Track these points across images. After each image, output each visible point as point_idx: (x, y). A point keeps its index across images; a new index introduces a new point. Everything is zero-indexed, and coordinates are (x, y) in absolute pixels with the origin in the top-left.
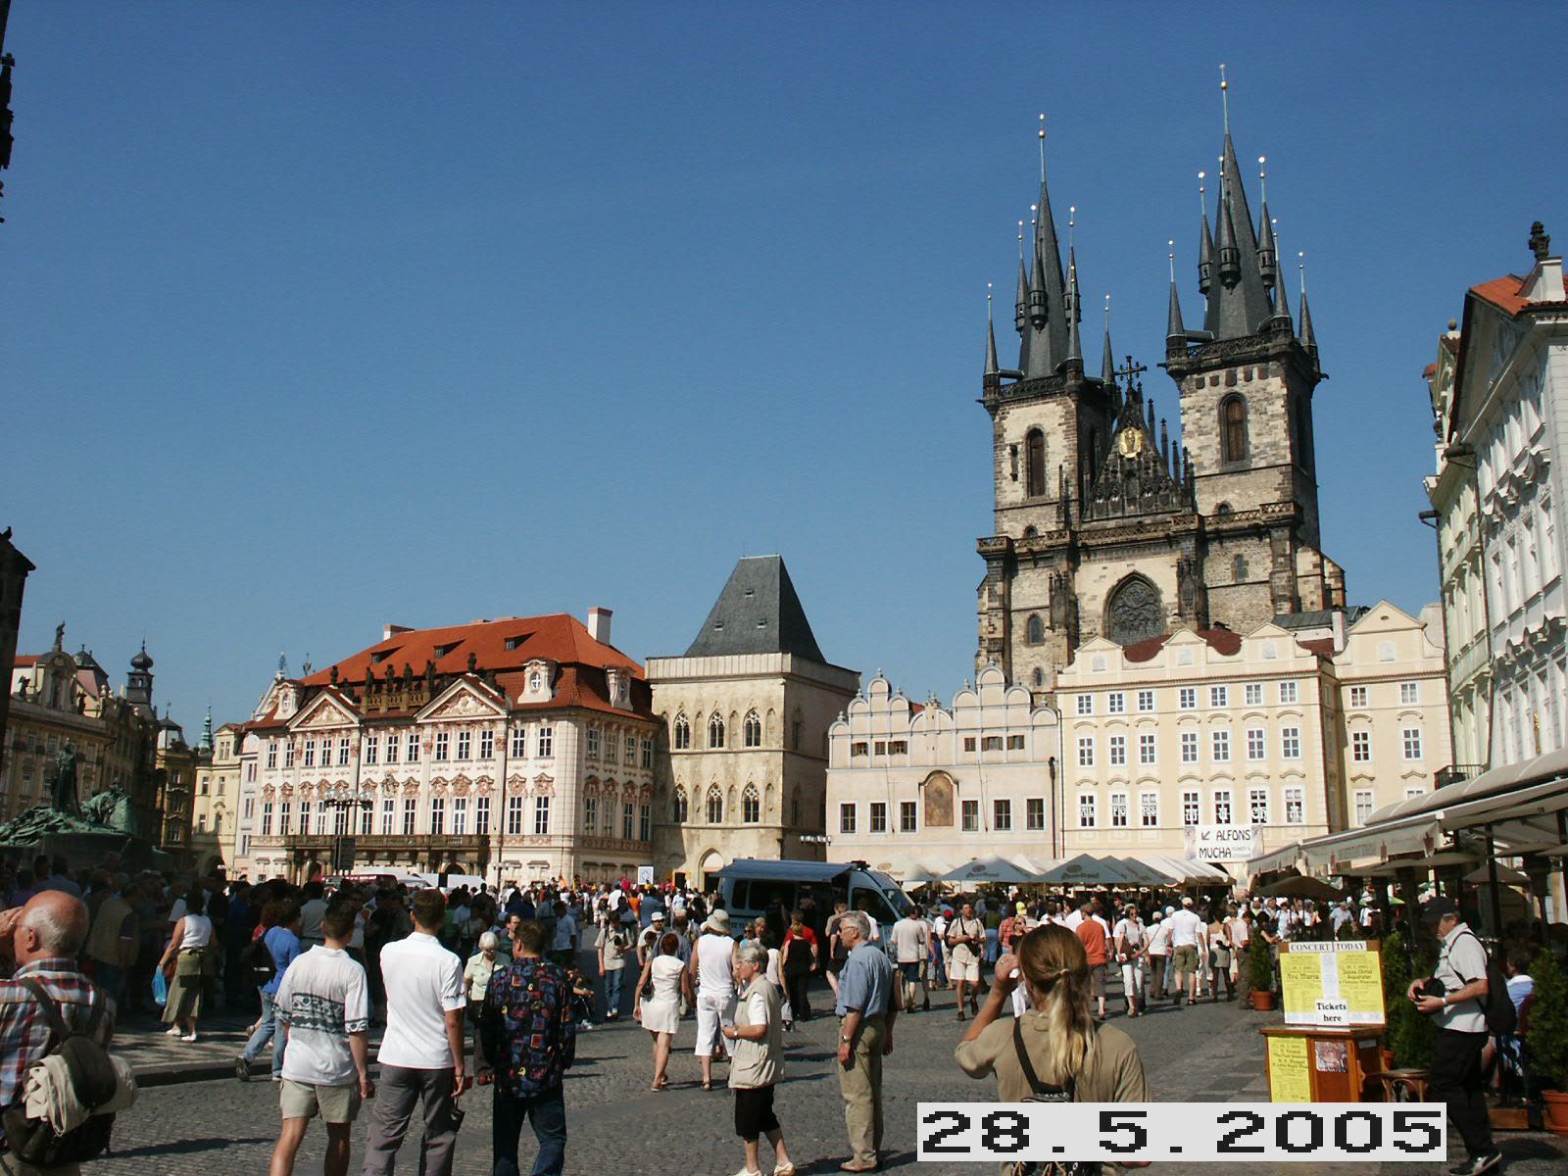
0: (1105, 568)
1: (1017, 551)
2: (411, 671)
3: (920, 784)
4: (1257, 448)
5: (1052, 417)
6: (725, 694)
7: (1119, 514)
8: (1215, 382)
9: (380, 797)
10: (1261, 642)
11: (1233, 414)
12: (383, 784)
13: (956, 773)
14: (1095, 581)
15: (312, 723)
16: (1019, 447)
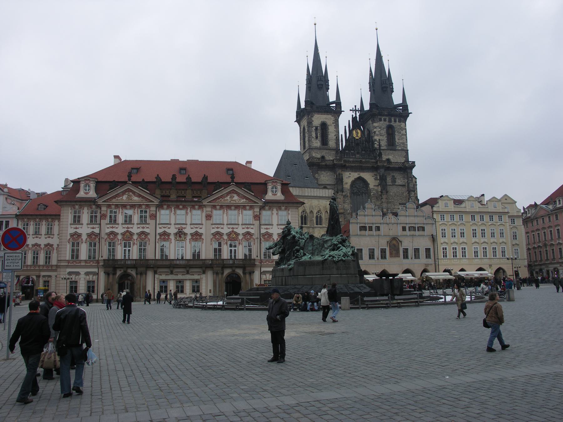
0: (350, 174)
1: (320, 164)
2: (191, 178)
3: (388, 242)
4: (398, 143)
5: (328, 119)
6: (307, 204)
7: (354, 157)
8: (385, 120)
9: (173, 241)
10: (493, 203)
11: (391, 132)
12: (176, 234)
13: (400, 239)
14: (347, 178)
15: (114, 200)
16: (318, 128)
